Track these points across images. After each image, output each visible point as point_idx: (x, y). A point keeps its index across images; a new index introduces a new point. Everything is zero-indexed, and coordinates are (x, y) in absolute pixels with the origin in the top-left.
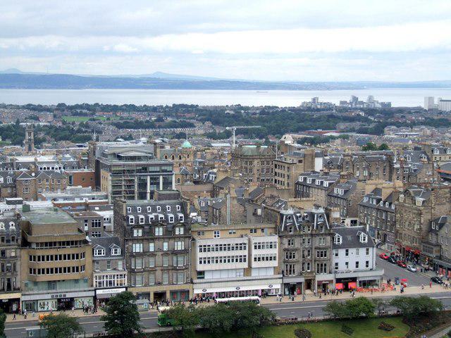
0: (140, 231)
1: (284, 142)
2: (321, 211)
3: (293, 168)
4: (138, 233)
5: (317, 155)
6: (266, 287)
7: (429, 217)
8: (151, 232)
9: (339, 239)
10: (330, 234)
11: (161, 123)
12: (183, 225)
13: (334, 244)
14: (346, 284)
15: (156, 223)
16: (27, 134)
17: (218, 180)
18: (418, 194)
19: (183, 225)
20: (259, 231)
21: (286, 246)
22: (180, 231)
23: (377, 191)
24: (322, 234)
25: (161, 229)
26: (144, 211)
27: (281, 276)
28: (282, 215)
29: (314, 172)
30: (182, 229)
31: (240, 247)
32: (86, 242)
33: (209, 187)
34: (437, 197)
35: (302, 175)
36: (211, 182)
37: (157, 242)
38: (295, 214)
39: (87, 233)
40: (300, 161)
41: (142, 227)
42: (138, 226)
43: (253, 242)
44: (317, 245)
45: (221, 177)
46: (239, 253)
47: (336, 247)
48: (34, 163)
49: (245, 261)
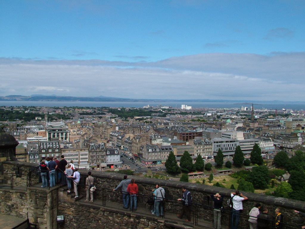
0: (44, 150)
1: (111, 121)
2: (103, 144)
3: (109, 130)
4: (43, 151)
5: (117, 126)
6: (85, 167)
7: (140, 145)
8: (48, 151)
9: (108, 153)
10: (105, 151)
11: (95, 113)
12: (58, 149)
13: (107, 154)
14: (110, 166)
15: (49, 148)
16: (45, 117)
17: (83, 134)
18: (137, 138)
19: (58, 149)
20: (83, 150)
21: (91, 155)
22: (57, 151)
23: (129, 138)
24: (103, 151)
25: (51, 150)
26: (46, 145)
27: (89, 164)
28: (90, 145)
29: (115, 131)
30: (58, 150)
31: (77, 155)
32: (28, 154)
33: (80, 136)
34: (142, 139)
35: (111, 132)
36: (81, 134)
37: (49, 154)
38: (94, 145)
39: (32, 151)
40: (111, 128)
41: (45, 149)
42: (43, 149)
43: (80, 154)
44: (101, 154)
45: (84, 133)
46: (76, 157)
47: (107, 155)
48: (30, 128)
49: (78, 159)
